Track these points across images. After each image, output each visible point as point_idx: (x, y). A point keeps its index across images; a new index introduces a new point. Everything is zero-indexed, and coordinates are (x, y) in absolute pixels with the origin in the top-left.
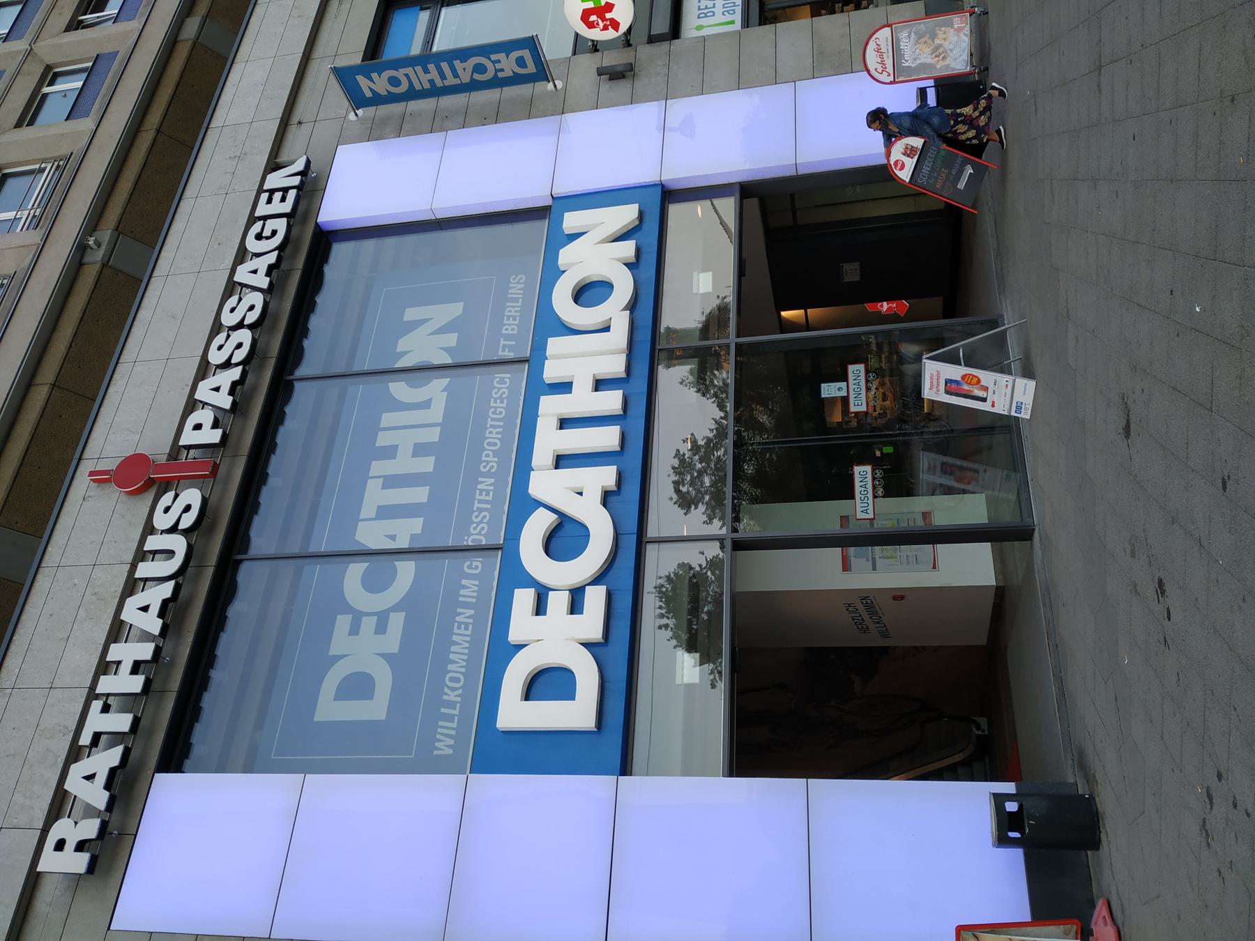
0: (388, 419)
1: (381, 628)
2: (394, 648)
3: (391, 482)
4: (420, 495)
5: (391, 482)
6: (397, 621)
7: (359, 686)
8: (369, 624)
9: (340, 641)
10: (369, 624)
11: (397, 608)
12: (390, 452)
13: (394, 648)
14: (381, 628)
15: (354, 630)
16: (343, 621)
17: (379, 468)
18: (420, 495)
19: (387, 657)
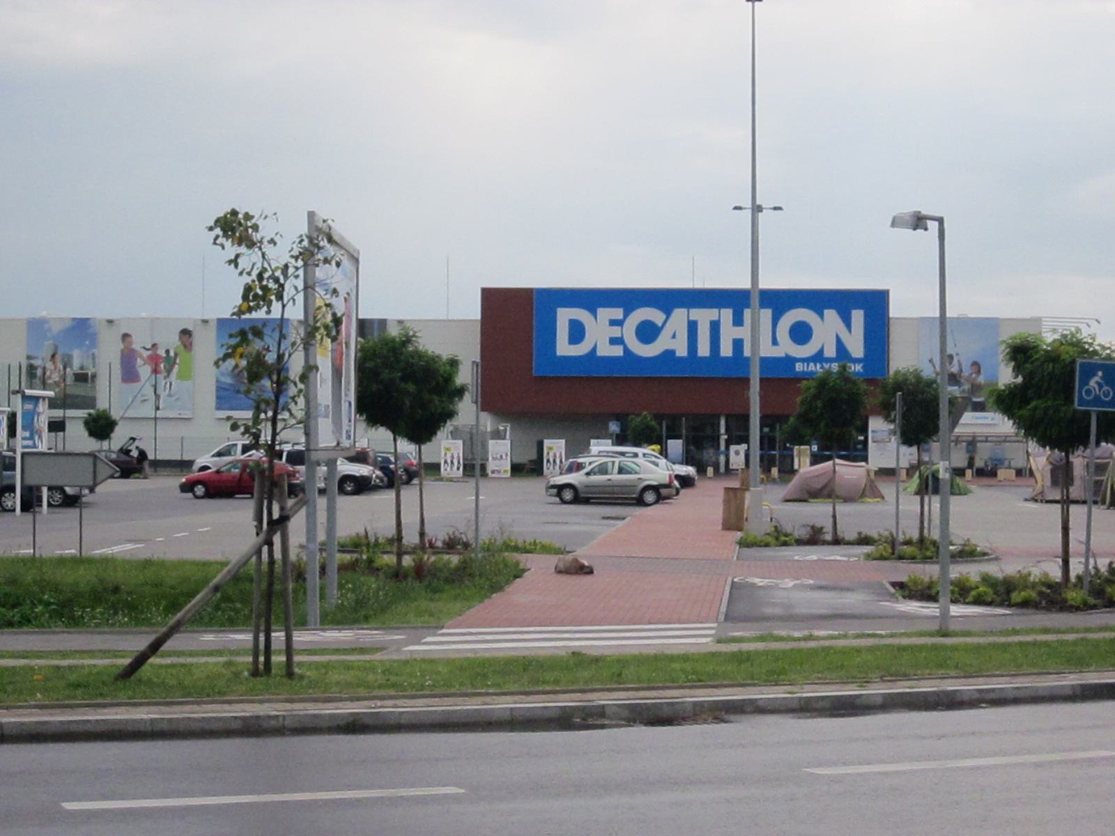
0: (766, 314)
1: (614, 341)
2: (600, 353)
3: (715, 327)
4: (704, 350)
5: (715, 327)
6: (618, 351)
7: (577, 333)
8: (616, 332)
9: (606, 314)
10: (616, 332)
11: (626, 350)
12: (738, 321)
13: (600, 353)
14: (614, 341)
15: (613, 323)
16: (618, 313)
17: (727, 315)
18: (704, 350)
19: (594, 349)
